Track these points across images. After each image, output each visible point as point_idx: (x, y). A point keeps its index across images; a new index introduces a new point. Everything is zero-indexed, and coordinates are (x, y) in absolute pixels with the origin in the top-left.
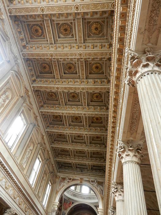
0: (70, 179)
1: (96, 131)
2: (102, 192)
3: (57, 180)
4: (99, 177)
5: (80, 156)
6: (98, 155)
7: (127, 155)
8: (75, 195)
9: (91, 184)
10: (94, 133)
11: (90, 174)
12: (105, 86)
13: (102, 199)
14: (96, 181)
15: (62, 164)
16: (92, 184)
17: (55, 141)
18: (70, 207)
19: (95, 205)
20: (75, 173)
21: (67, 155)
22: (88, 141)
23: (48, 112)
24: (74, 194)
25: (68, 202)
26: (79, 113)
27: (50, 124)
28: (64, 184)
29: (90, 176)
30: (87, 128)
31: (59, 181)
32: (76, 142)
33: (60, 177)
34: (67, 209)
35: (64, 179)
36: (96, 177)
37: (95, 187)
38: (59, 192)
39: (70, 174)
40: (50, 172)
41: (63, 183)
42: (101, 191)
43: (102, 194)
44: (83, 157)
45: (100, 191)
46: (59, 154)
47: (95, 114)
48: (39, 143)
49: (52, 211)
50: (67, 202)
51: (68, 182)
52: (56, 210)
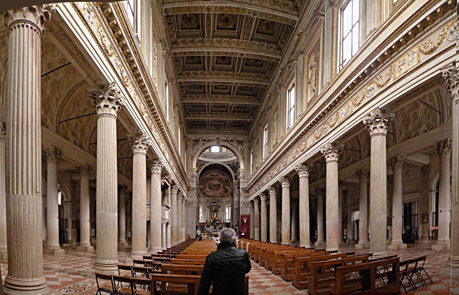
1: (250, 78)
2: (243, 152)
4: (239, 135)
9: (230, 144)
10: (247, 82)
13: (244, 159)
14: (235, 140)
16: (232, 144)
21: (200, 111)
26: (233, 52)
27: (183, 71)
29: (227, 134)
39: (202, 134)
42: (242, 151)
43: (243, 154)
46: (190, 111)
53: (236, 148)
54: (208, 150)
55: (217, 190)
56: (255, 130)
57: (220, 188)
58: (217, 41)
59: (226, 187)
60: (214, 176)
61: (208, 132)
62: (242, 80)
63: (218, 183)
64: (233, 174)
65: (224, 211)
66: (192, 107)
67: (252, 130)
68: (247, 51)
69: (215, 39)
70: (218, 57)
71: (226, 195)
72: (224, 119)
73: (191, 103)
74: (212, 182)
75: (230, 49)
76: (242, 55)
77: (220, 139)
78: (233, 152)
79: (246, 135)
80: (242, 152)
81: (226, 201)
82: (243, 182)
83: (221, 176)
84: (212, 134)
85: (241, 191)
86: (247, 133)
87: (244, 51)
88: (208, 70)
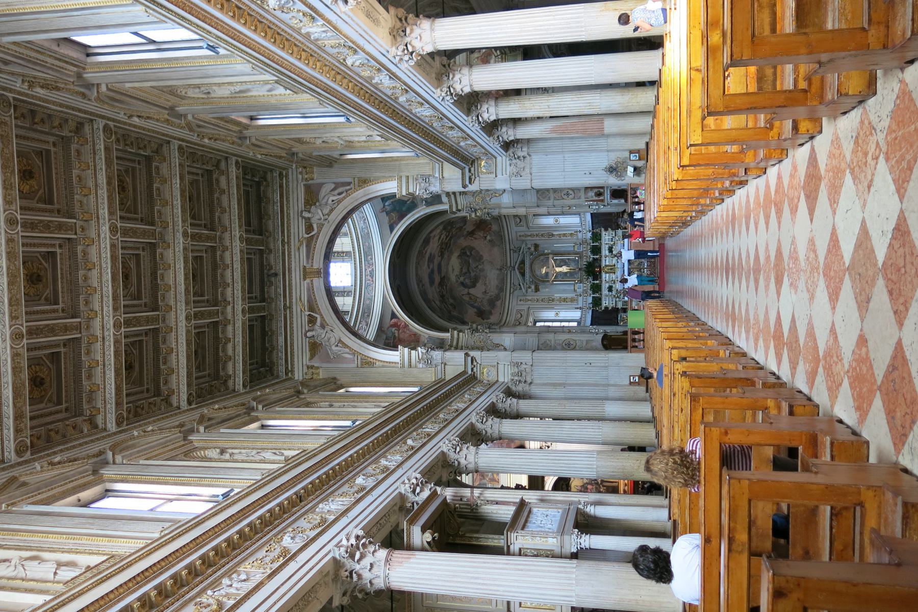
0: (312, 320)
1: (91, 184)
3: (322, 375)
4: (288, 201)
5: (214, 276)
6: (199, 195)
8: (364, 313)
9: (319, 233)
10: (103, 192)
11: (283, 241)
13: (364, 182)
14: (306, 215)
15: (255, 366)
16: (321, 226)
17: (158, 393)
18: (406, 326)
21: (217, 339)
22: (144, 234)
23: (18, 417)
25: (394, 333)
26: (8, 253)
28: (333, 340)
29: (289, 242)
30: (83, 229)
31: (324, 365)
32: (155, 288)
33: (308, 367)
34: (415, 335)
35: (315, 347)
36: (288, 214)
37: (329, 215)
38: (366, 353)
40: (298, 397)
42: (340, 190)
43: (349, 184)
44: (215, 267)
45: (340, 194)
46: (217, 377)
52: (424, 351)
53: (332, 210)
54: (346, 303)
55: (481, 257)
56: (264, 151)
57: (472, 249)
59: (469, 227)
61: (285, 310)
62: (101, 211)
63: (456, 254)
64: (421, 212)
65: (549, 233)
66: (204, 370)
67: (269, 160)
70: (29, 299)
71: (495, 227)
72: (237, 258)
74: (453, 278)
77: (304, 267)
78: (344, 219)
79: (287, 176)
80: (343, 187)
81: (517, 225)
84: (290, 293)
85: (471, 188)
86: (281, 174)
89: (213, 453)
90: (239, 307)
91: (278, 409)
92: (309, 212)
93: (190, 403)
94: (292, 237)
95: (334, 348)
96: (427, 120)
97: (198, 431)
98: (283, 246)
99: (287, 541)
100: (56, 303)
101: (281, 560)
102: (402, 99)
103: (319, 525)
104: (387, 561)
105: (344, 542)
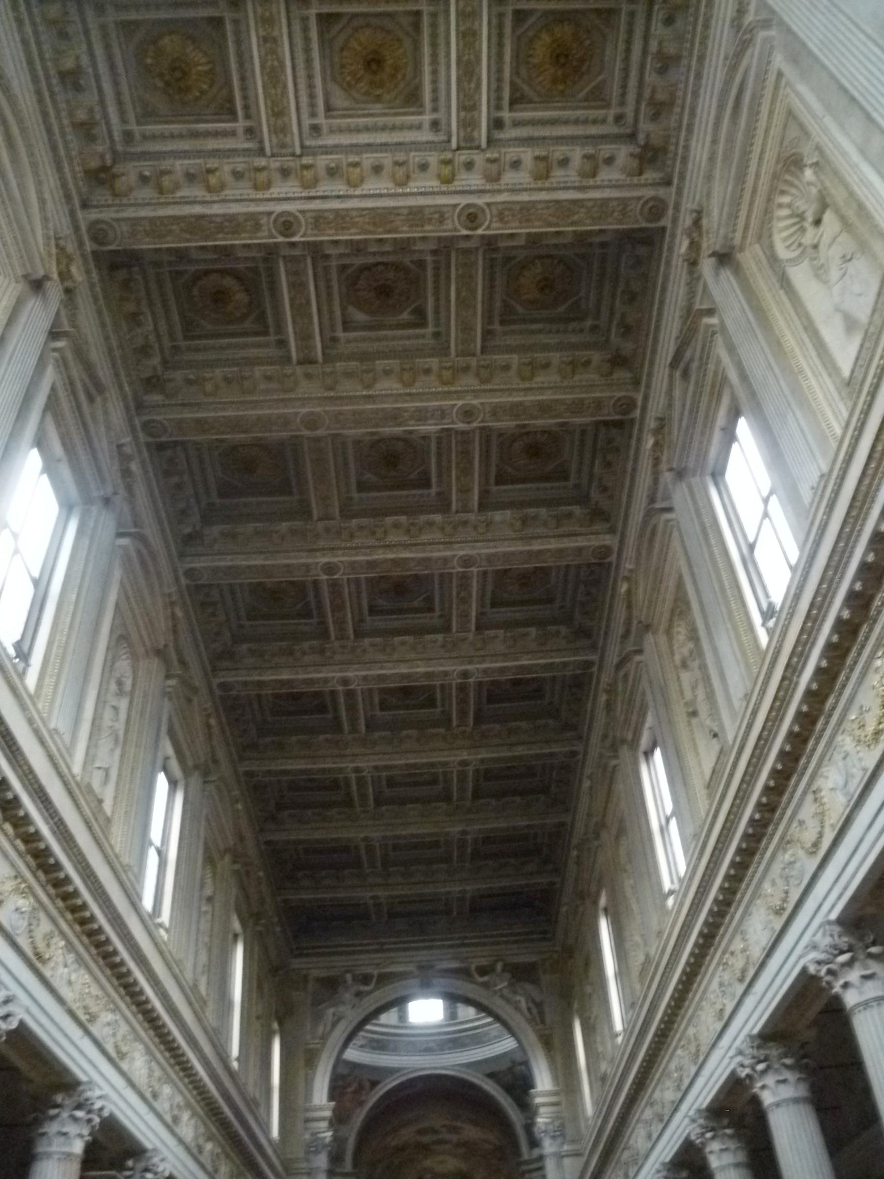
0: (366, 979)
2: (541, 1014)
4: (516, 942)
7: (866, 978)
8: (378, 1041)
12: (581, 542)
13: (547, 1043)
16: (485, 985)
17: (280, 807)
18: (361, 1104)
19: (488, 1071)
20: (382, 944)
22: (462, 789)
23: (260, 684)
24: (372, 1040)
28: (342, 1009)
32: (402, 802)
36: (498, 943)
41: (333, 1006)
42: (535, 1011)
43: (543, 1021)
45: (529, 1009)
47: (516, 666)
48: (226, 851)
49: (308, 1152)
50: (344, 1088)
51: (359, 994)
53: (508, 1001)
54: (389, 1018)
58: (373, 645)
60: (436, 1132)
63: (464, 1166)
68: (484, 662)
69: (367, 641)
70: (383, 691)
73: (300, 842)
74: (428, 1163)
75: (419, 662)
76: (465, 674)
78: (498, 1018)
79: (544, 939)
82: (560, 1157)
83: (471, 1132)
87: (470, 663)
88: (354, 729)
89: (208, 891)
90: (381, 893)
91: (256, 949)
92: (503, 970)
93: (268, 843)
94: (470, 949)
95: (331, 1011)
96: (631, 1142)
97: (234, 862)
98: (458, 939)
99: (107, 1017)
100: (382, 709)
101: (83, 1018)
102: (648, 1114)
103: (119, 1052)
104: (69, 1156)
105: (98, 1093)
